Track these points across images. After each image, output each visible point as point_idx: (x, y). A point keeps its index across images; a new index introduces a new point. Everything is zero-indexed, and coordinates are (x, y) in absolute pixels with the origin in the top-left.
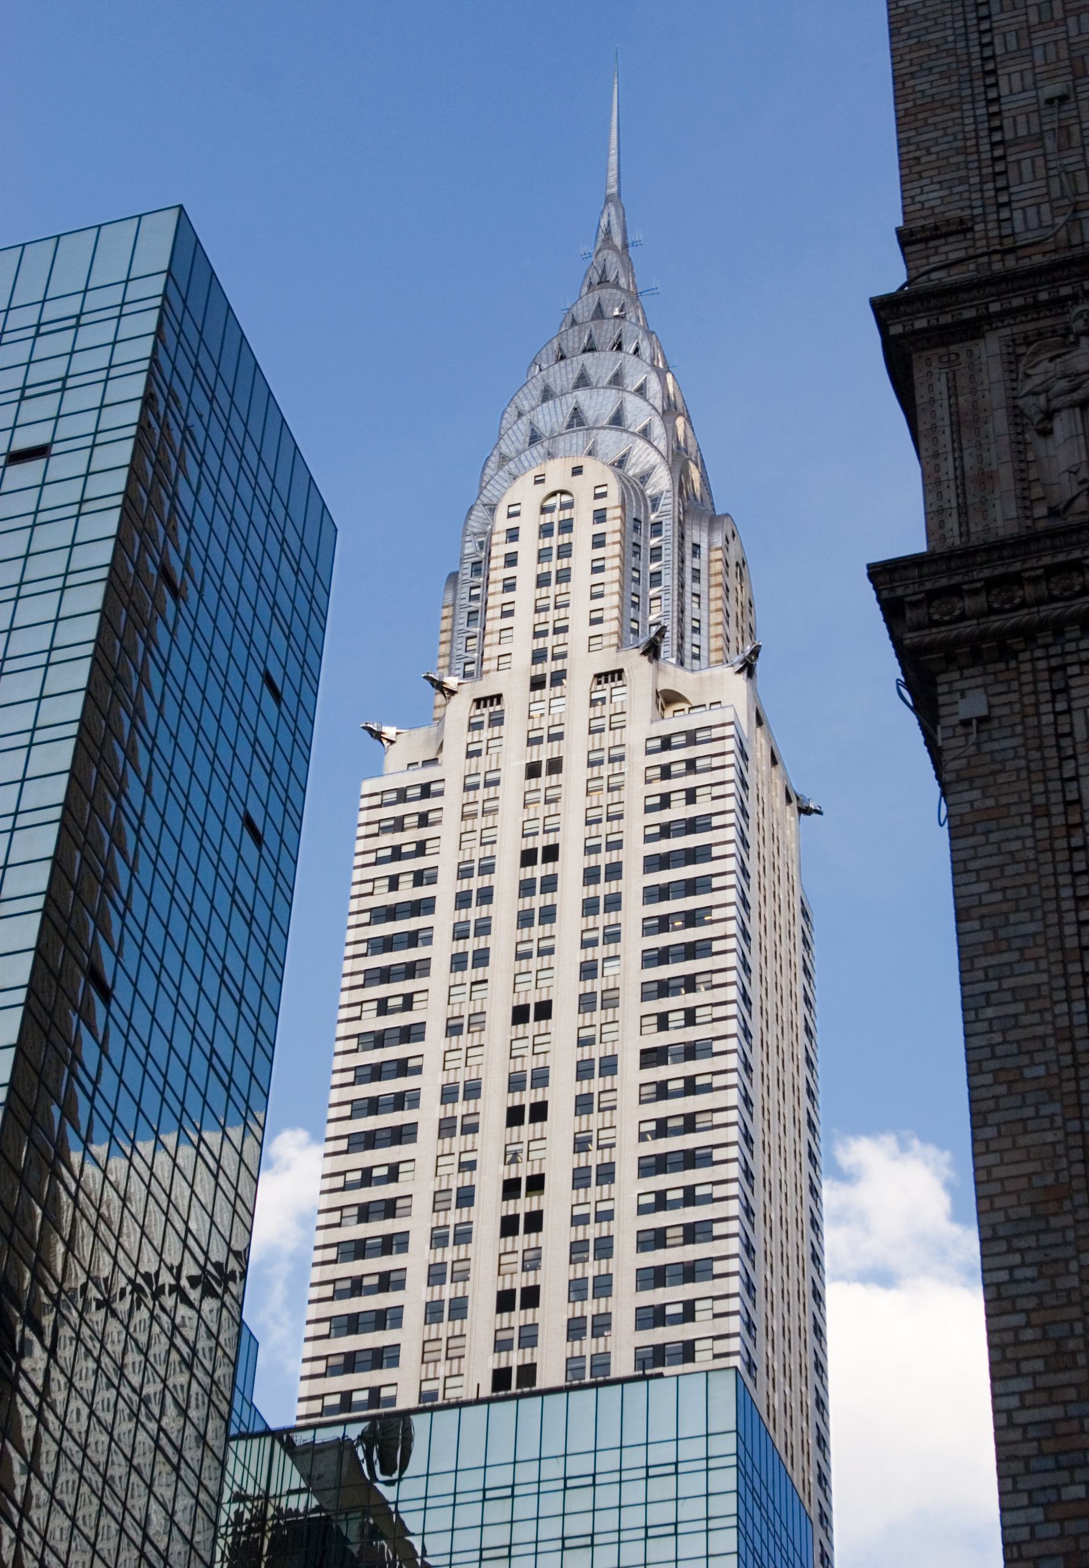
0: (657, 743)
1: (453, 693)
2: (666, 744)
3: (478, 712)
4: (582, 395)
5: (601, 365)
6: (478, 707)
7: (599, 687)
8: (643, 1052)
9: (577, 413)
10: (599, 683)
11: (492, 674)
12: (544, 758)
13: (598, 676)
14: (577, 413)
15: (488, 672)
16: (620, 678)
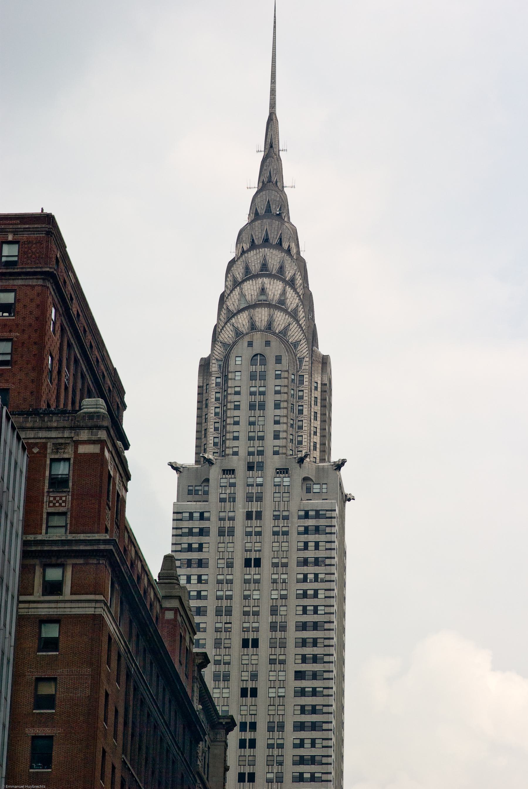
0: (302, 513)
1: (213, 464)
2: (306, 516)
3: (224, 476)
4: (266, 280)
5: (274, 258)
6: (224, 474)
7: (278, 475)
8: (296, 672)
9: (263, 291)
10: (278, 473)
11: (230, 456)
12: (254, 510)
13: (277, 469)
14: (263, 291)
15: (228, 455)
16: (287, 473)
